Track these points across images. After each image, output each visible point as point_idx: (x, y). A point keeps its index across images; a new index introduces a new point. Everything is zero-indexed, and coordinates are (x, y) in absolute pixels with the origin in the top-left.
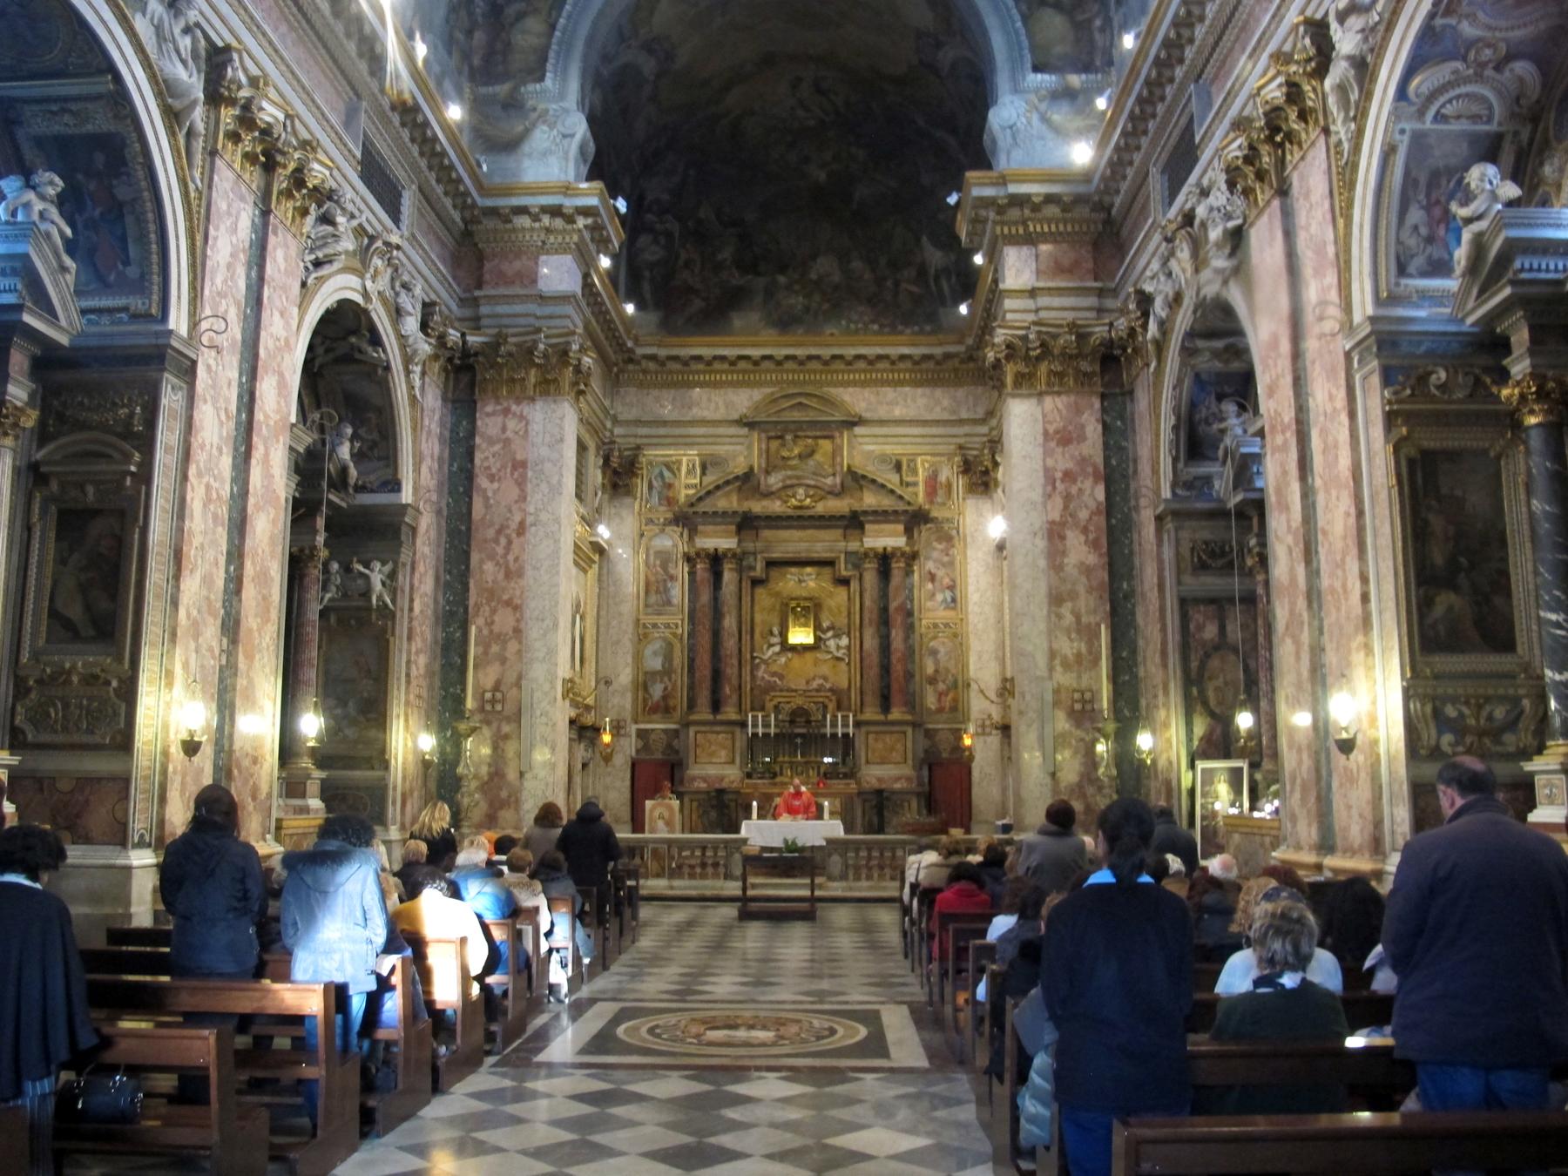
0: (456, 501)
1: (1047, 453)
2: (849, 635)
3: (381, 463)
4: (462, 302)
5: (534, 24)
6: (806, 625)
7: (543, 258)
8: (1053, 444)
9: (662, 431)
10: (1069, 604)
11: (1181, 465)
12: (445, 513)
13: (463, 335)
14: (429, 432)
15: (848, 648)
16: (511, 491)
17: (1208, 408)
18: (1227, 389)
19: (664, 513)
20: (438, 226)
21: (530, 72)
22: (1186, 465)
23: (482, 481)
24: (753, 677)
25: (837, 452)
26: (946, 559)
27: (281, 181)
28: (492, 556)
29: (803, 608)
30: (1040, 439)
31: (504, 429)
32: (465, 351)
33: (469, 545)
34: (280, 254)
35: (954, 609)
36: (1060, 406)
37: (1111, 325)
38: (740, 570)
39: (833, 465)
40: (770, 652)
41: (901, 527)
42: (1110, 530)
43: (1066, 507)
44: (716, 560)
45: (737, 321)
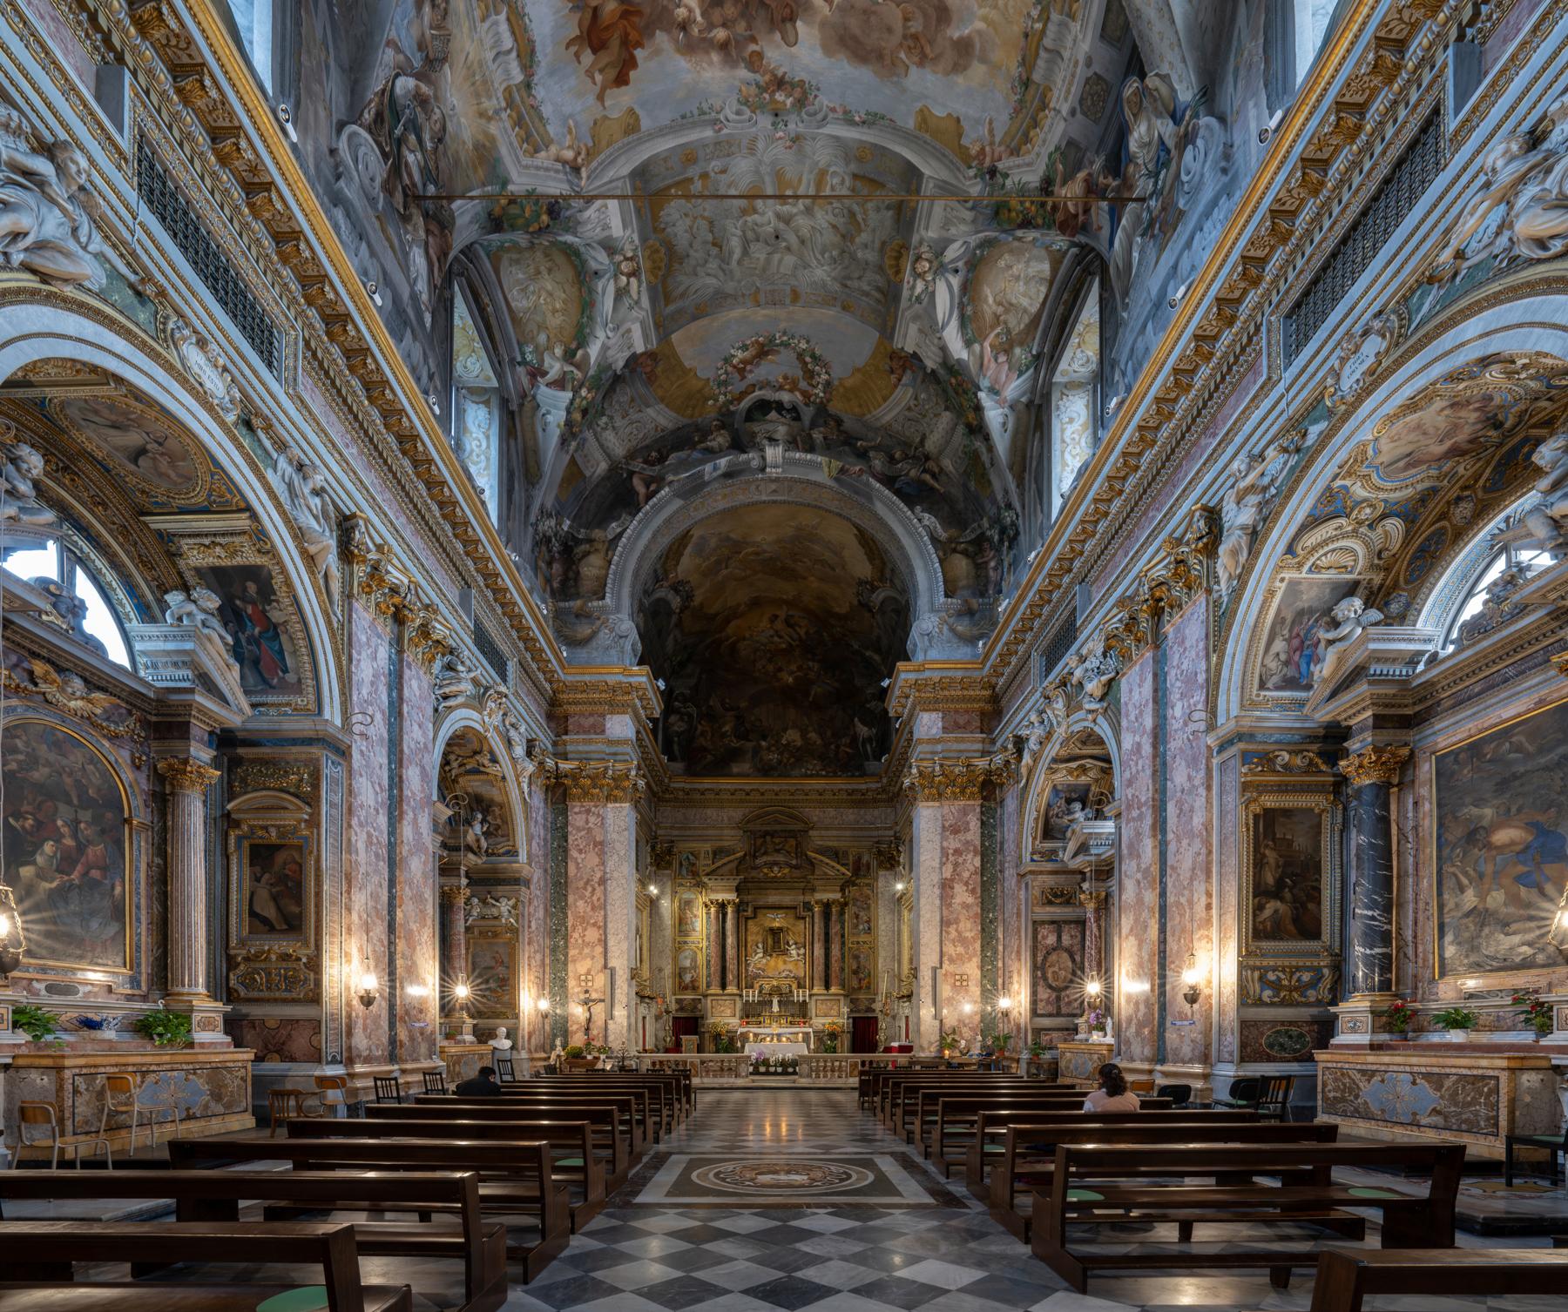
1: (944, 838)
18: (1074, 796)
21: (595, 593)
27: (410, 632)
34: (414, 683)
42: (983, 883)
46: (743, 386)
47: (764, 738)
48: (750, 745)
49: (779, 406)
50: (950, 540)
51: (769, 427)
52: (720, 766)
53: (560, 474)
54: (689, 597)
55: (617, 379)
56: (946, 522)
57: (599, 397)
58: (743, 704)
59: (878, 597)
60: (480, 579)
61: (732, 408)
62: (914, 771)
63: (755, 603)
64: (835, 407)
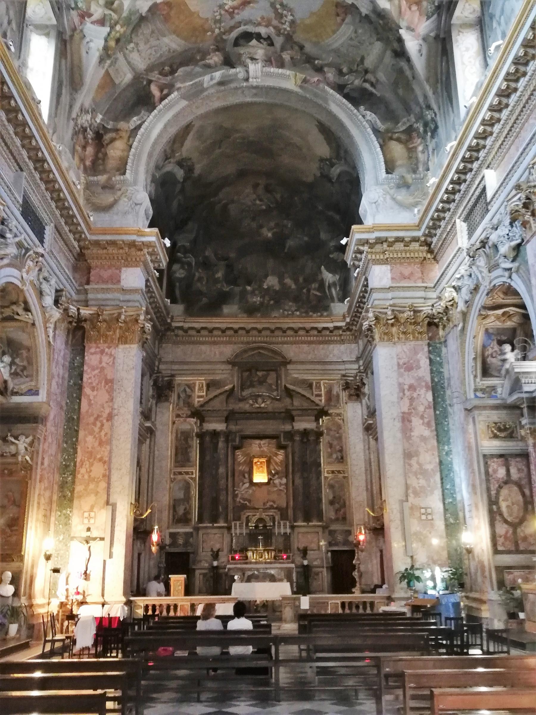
0: (72, 402)
1: (401, 375)
2: (287, 477)
3: (28, 379)
4: (78, 292)
5: (119, 145)
6: (263, 472)
7: (124, 269)
8: (402, 370)
9: (186, 367)
10: (415, 458)
11: (478, 380)
12: (65, 408)
13: (78, 309)
14: (57, 363)
15: (286, 484)
16: (102, 396)
17: (492, 348)
18: (504, 338)
19: (186, 411)
20: (65, 248)
22: (481, 380)
23: (87, 390)
24: (234, 501)
25: (278, 377)
26: (337, 435)
28: (91, 433)
29: (261, 463)
30: (396, 368)
31: (101, 362)
32: (80, 320)
33: (78, 426)
35: (342, 462)
36: (406, 350)
37: (433, 306)
38: (227, 441)
39: (277, 386)
40: (243, 488)
41: (313, 418)
43: (411, 405)
44: (215, 434)
45: (226, 309)
46: (232, 23)
47: (249, 284)
48: (237, 289)
49: (258, 37)
50: (387, 131)
51: (251, 50)
52: (214, 307)
53: (97, 83)
54: (190, 170)
55: (142, 19)
56: (384, 119)
57: (129, 32)
58: (232, 255)
59: (336, 171)
60: (31, 165)
61: (224, 37)
62: (371, 315)
63: (242, 174)
64: (299, 37)
